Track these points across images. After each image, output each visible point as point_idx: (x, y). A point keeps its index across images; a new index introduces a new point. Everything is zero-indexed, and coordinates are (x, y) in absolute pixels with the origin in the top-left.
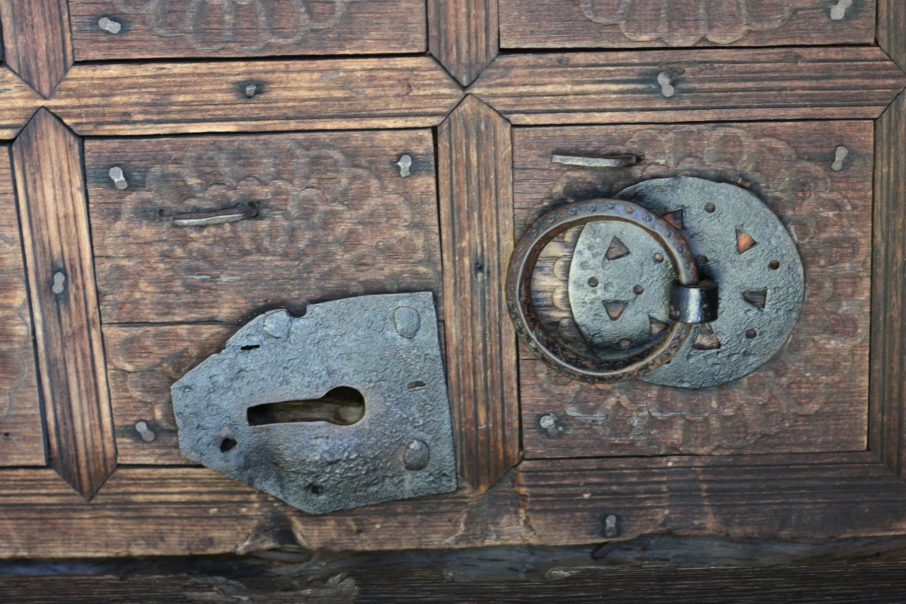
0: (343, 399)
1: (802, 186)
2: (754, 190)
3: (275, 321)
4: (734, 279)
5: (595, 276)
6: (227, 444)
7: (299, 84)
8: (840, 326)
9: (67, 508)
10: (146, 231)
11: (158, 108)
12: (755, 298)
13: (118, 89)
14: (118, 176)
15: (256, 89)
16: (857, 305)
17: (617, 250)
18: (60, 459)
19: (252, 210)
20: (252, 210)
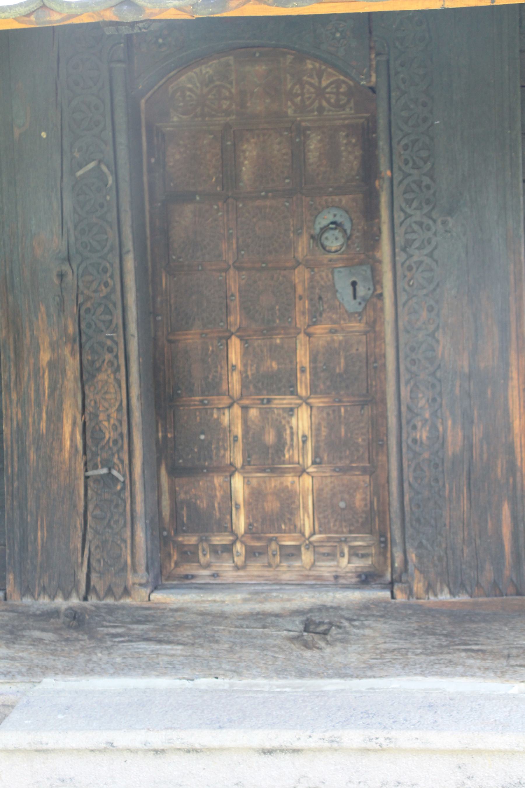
0: (354, 284)
1: (316, 209)
2: (316, 217)
3: (338, 295)
4: (331, 218)
5: (334, 241)
6: (360, 304)
7: (300, 290)
8: (340, 201)
9: (375, 332)
10: (324, 315)
11: (303, 313)
12: (335, 216)
13: (301, 321)
14: (314, 320)
15: (301, 298)
16: (337, 198)
17: (327, 238)
18: (366, 333)
19: (320, 298)
20: (320, 298)
